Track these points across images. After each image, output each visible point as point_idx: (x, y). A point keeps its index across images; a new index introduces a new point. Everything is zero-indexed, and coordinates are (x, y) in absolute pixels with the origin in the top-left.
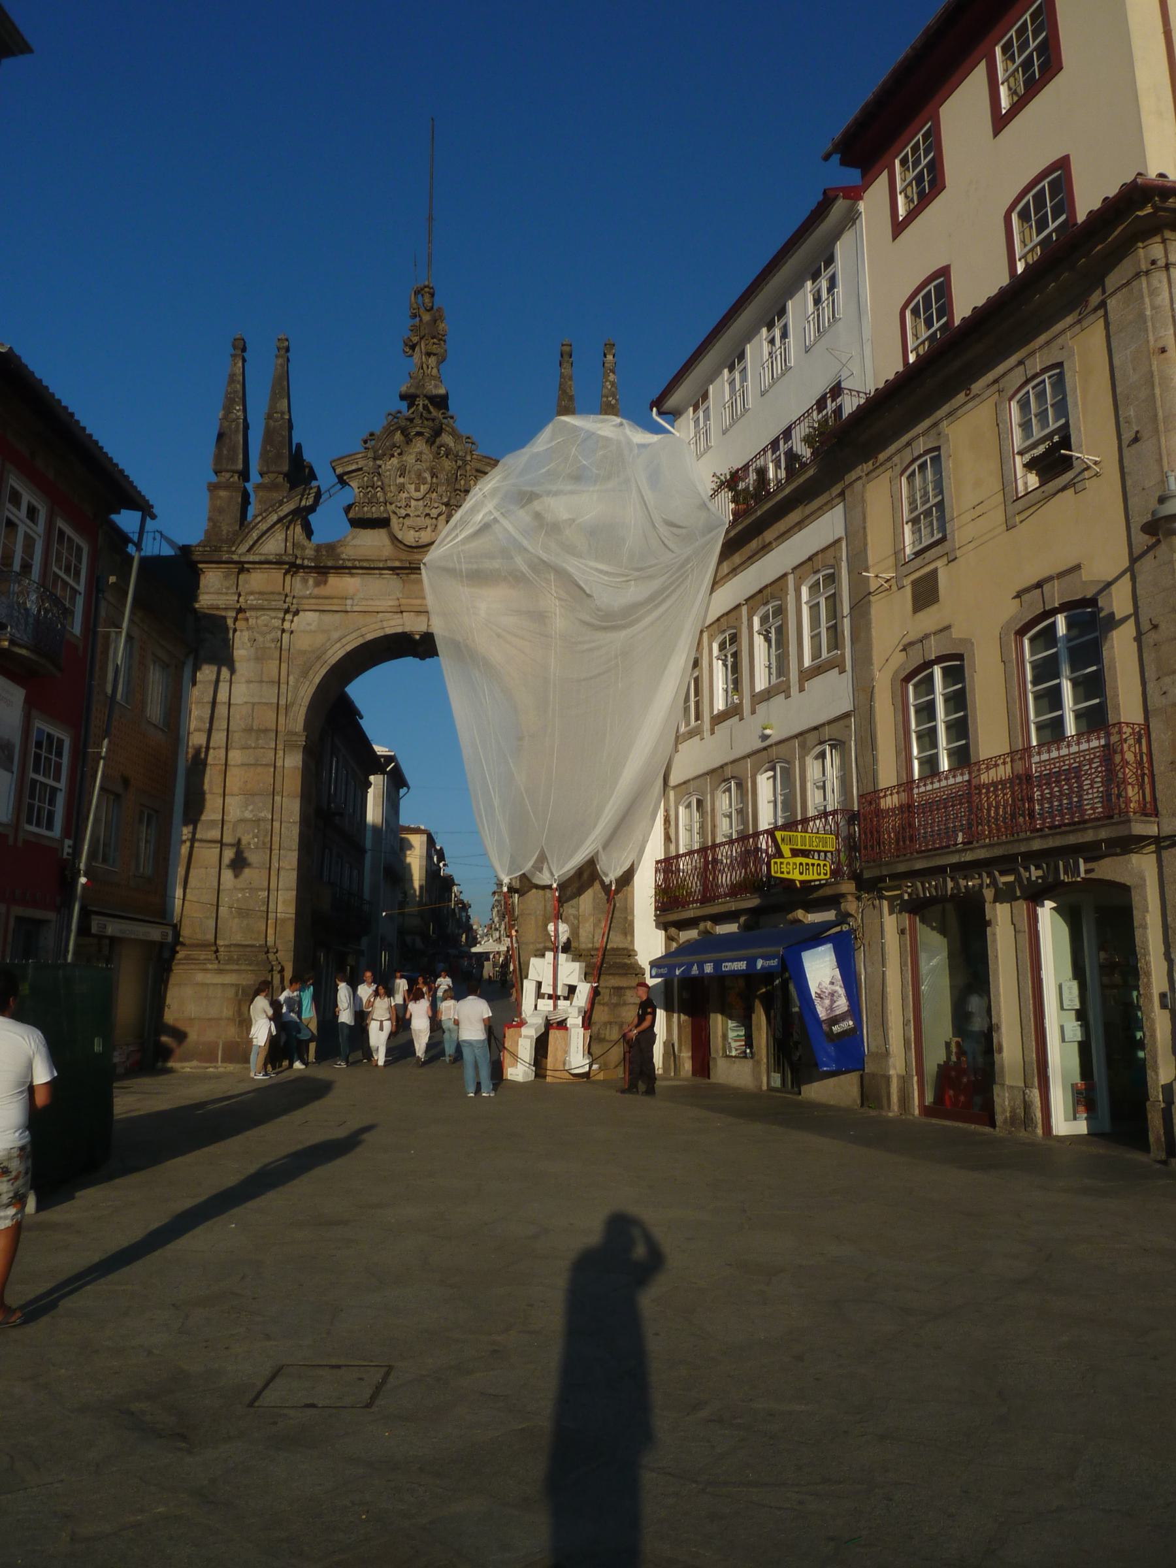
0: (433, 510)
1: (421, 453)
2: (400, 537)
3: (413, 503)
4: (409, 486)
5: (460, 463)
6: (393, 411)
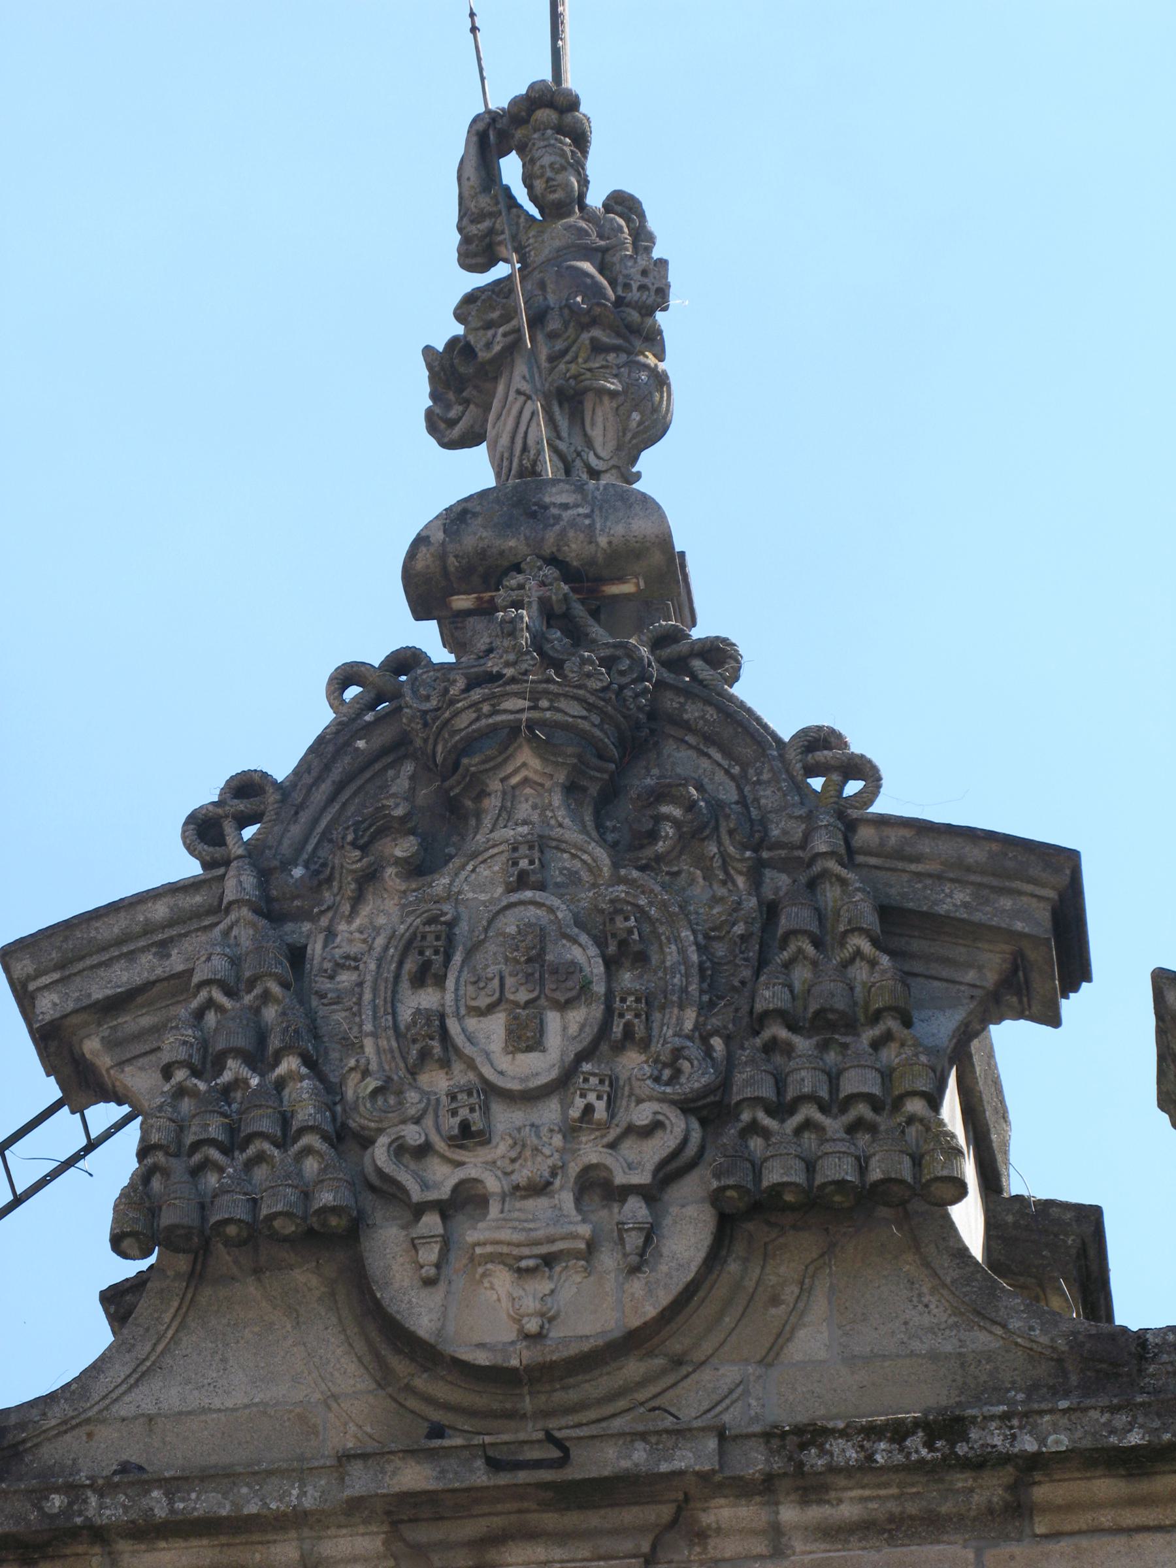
0: (630, 1149)
1: (542, 844)
2: (424, 1324)
3: (505, 1118)
4: (472, 1023)
5: (778, 881)
6: (376, 659)
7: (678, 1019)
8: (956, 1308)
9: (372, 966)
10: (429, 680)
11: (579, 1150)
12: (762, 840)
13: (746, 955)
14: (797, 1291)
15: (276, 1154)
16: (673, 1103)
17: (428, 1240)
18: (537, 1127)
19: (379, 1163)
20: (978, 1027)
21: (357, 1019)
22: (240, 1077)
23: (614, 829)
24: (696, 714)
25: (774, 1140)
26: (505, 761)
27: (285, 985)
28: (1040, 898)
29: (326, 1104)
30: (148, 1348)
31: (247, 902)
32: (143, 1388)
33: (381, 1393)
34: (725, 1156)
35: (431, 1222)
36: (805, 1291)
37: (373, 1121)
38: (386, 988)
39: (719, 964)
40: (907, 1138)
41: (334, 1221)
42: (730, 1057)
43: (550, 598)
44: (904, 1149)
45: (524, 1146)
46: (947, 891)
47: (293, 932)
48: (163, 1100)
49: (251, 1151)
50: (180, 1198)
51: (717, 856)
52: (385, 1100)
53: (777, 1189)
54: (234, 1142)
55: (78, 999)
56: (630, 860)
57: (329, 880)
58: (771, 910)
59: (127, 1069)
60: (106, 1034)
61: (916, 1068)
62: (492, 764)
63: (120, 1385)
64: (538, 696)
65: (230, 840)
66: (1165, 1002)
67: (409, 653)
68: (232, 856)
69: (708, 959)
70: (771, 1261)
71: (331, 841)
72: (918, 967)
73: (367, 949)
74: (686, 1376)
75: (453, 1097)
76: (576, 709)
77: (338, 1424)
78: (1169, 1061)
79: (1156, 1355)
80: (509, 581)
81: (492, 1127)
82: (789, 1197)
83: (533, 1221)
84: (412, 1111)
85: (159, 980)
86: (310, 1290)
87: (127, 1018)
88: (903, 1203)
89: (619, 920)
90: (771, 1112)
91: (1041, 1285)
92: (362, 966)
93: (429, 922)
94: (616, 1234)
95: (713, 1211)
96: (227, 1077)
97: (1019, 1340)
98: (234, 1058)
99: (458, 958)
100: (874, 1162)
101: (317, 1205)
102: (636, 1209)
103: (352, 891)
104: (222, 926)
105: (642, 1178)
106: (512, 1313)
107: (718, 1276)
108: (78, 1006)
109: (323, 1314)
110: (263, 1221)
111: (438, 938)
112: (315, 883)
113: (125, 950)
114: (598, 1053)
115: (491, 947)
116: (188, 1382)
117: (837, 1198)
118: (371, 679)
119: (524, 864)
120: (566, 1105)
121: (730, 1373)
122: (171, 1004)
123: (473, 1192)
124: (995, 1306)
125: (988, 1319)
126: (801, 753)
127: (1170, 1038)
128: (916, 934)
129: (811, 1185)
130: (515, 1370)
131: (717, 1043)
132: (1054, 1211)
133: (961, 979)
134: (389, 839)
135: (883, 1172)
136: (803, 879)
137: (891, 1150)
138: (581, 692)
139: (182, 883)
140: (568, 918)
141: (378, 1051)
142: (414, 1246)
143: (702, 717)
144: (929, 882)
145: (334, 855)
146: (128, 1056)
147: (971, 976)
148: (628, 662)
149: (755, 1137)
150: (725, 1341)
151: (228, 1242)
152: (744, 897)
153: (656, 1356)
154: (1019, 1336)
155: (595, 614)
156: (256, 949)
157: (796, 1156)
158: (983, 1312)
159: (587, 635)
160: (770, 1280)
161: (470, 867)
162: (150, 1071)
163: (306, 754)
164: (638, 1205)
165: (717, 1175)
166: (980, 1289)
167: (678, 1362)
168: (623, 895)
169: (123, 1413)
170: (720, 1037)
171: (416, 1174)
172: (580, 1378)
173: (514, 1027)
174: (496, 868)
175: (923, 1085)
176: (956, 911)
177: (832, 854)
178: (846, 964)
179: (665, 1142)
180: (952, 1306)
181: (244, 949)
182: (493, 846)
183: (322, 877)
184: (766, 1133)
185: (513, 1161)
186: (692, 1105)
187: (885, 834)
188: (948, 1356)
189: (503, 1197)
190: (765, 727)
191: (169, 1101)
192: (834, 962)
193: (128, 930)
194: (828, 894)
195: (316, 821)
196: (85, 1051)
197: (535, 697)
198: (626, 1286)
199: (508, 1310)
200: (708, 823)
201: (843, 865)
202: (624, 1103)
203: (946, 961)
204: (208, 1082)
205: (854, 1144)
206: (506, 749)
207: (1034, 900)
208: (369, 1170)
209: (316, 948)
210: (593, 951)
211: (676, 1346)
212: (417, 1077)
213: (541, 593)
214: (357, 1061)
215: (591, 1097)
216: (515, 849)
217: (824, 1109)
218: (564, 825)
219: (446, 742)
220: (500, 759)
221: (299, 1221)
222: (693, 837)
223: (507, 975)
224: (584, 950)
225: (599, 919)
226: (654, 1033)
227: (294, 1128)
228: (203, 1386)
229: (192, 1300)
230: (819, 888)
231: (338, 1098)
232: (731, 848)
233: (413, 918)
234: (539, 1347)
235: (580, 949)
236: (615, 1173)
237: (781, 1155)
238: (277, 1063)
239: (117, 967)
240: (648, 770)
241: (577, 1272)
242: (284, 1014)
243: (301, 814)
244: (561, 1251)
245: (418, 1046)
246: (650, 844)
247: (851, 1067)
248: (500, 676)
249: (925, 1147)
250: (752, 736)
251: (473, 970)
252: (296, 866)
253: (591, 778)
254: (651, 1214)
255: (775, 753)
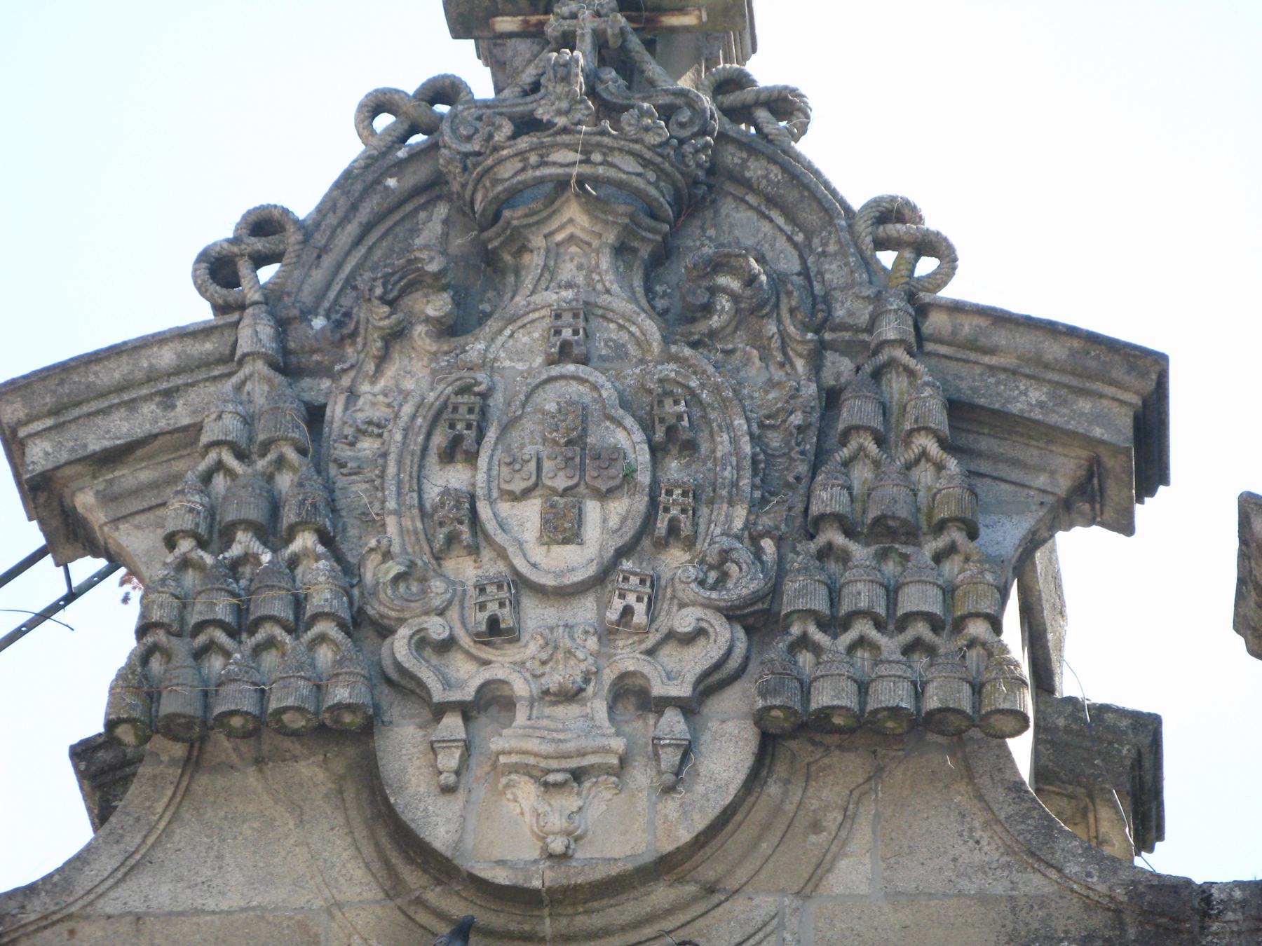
0: (670, 656)
1: (587, 311)
3: (536, 615)
4: (504, 508)
5: (840, 367)
6: (410, 84)
7: (727, 516)
8: (1009, 846)
9: (398, 437)
10: (470, 119)
11: (615, 655)
12: (825, 320)
13: (802, 447)
14: (840, 818)
15: (287, 641)
16: (719, 609)
17: (449, 744)
18: (572, 627)
19: (399, 657)
20: (1046, 535)
21: (380, 494)
22: (251, 552)
23: (665, 294)
24: (759, 172)
25: (825, 657)
26: (550, 216)
27: (302, 451)
28: (1122, 403)
29: (344, 589)
30: (138, 840)
31: (264, 356)
32: (131, 884)
33: (389, 904)
34: (772, 673)
35: (452, 724)
36: (849, 818)
37: (393, 610)
38: (412, 461)
39: (773, 455)
40: (968, 663)
41: (348, 718)
42: (781, 559)
43: (605, 32)
44: (965, 676)
45: (556, 648)
46: (1022, 388)
47: (311, 389)
48: (166, 573)
49: (261, 635)
50: (182, 685)
51: (776, 336)
52: (407, 587)
53: (826, 713)
54: (242, 625)
55: (73, 450)
56: (682, 335)
57: (353, 335)
58: (832, 398)
59: (121, 527)
60: (101, 488)
61: (980, 587)
62: (535, 218)
63: (106, 879)
64: (590, 148)
65: (246, 283)
66: (1251, 528)
67: (447, 82)
68: (248, 302)
69: (761, 449)
70: (814, 783)
71: (355, 288)
72: (985, 467)
73: (392, 416)
74: (718, 905)
75: (482, 590)
76: (630, 165)
77: (341, 935)
78: (1251, 587)
79: (1220, 912)
80: (560, 8)
81: (522, 624)
82: (838, 720)
83: (563, 731)
84: (437, 603)
85: (162, 434)
86: (316, 785)
87: (125, 472)
88: (959, 733)
89: (668, 402)
90: (823, 626)
91: (1091, 797)
92: (386, 435)
93: (461, 391)
94: (650, 748)
95: (756, 729)
96: (236, 551)
97: (1075, 886)
98: (245, 530)
99: (491, 435)
100: (931, 689)
101: (331, 701)
102: (673, 723)
103: (378, 350)
104: (235, 380)
105: (683, 690)
106: (536, 829)
107: (758, 798)
108: (74, 457)
109: (329, 812)
110: (271, 714)
111: (471, 411)
112: (338, 336)
113: (126, 397)
114: (639, 548)
115: (528, 425)
116: (180, 879)
117: (890, 724)
118: (405, 109)
119: (567, 333)
120: (603, 606)
121: (765, 904)
122: (174, 459)
123: (499, 693)
124: (1052, 848)
125: (1043, 861)
126: (872, 225)
127: (1253, 564)
128: (986, 431)
129: (862, 710)
130: (536, 892)
131: (768, 545)
132: (1109, 717)
133: (1032, 484)
134: (420, 293)
135: (940, 700)
136: (868, 368)
137: (950, 677)
138: (637, 147)
139: (191, 329)
140: (613, 398)
141: (402, 531)
142: (433, 749)
143: (766, 177)
144: (1003, 376)
145: (360, 308)
146: (124, 512)
147: (1042, 480)
148: (689, 113)
149: (804, 651)
150: (760, 868)
151: (231, 734)
152: (802, 382)
153: (688, 882)
154: (1075, 882)
155: (650, 45)
156: (272, 409)
157: (849, 677)
158: (1038, 853)
159: (642, 72)
160: (812, 804)
161: (507, 332)
162: (147, 531)
163: (331, 190)
164: (676, 719)
165: (763, 694)
166: (1036, 827)
167: (711, 890)
168: (673, 375)
169: (109, 910)
170: (772, 538)
171: (438, 670)
172: (605, 902)
173: (551, 516)
174: (536, 335)
175: (986, 607)
176: (1031, 411)
177: (901, 342)
178: (909, 466)
179: (708, 652)
180: (1004, 843)
181: (258, 407)
182: (534, 310)
183: (346, 331)
184: (817, 649)
185: (544, 663)
186: (738, 612)
187: (958, 321)
188: (997, 899)
189: (532, 702)
190: (834, 192)
191: (172, 574)
192: (898, 463)
193: (131, 377)
194: (894, 386)
195: (339, 266)
196: (77, 505)
197: (587, 152)
198: (660, 807)
199: (532, 826)
200: (768, 300)
201: (912, 355)
202: (666, 606)
203: (1015, 463)
204: (215, 554)
205: (910, 667)
206: (553, 202)
207: (1116, 404)
208: (387, 663)
209: (336, 411)
210: (639, 436)
211: (709, 873)
212: (442, 562)
213: (596, 24)
214: (379, 541)
215: (631, 599)
216: (558, 316)
217: (879, 625)
218: (612, 291)
219: (487, 190)
220: (544, 214)
221: (309, 716)
222: (752, 312)
223: (544, 455)
224: (629, 434)
225: (647, 399)
226: (700, 530)
227: (308, 614)
228: (196, 885)
229: (187, 789)
230: (884, 378)
231: (355, 581)
232: (792, 327)
233: (443, 386)
234: (563, 868)
235: (625, 433)
236: (653, 683)
237: (832, 675)
238: (290, 538)
239: (117, 416)
240: (703, 230)
241: (607, 788)
242: (301, 485)
243: (324, 257)
244: (592, 766)
245: (445, 530)
246: (704, 317)
247: (911, 582)
248: (550, 124)
249: (987, 676)
250: (819, 202)
251: (508, 449)
252: (316, 315)
253: (643, 239)
254: (689, 728)
255: (843, 223)
